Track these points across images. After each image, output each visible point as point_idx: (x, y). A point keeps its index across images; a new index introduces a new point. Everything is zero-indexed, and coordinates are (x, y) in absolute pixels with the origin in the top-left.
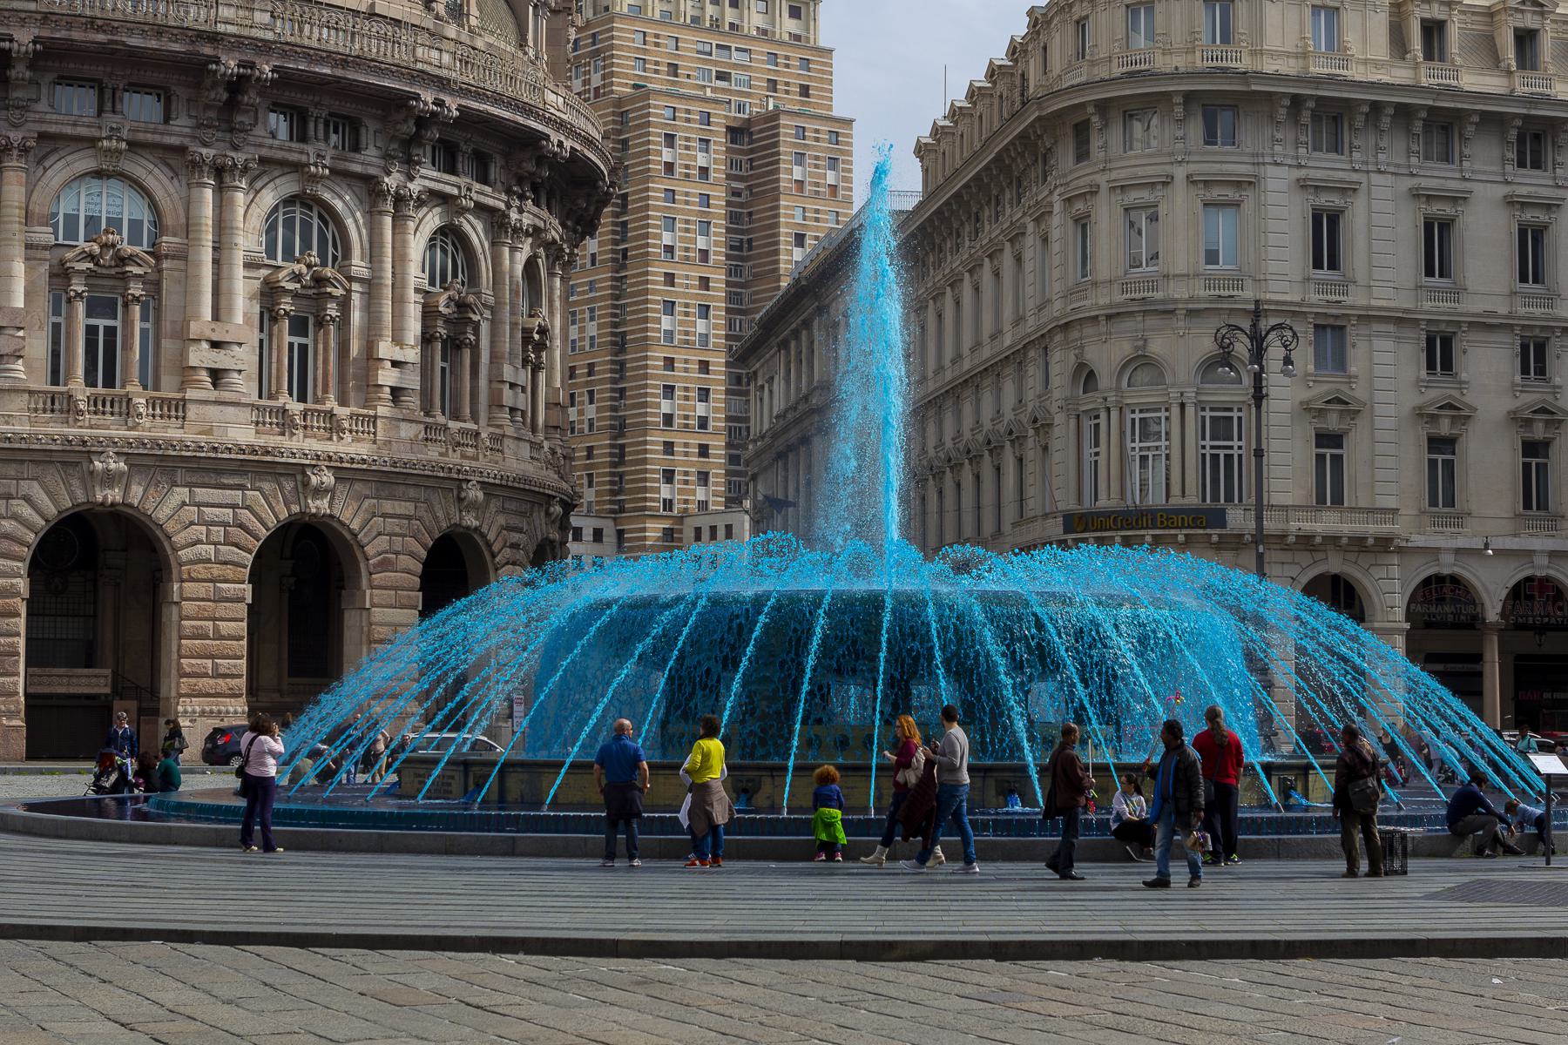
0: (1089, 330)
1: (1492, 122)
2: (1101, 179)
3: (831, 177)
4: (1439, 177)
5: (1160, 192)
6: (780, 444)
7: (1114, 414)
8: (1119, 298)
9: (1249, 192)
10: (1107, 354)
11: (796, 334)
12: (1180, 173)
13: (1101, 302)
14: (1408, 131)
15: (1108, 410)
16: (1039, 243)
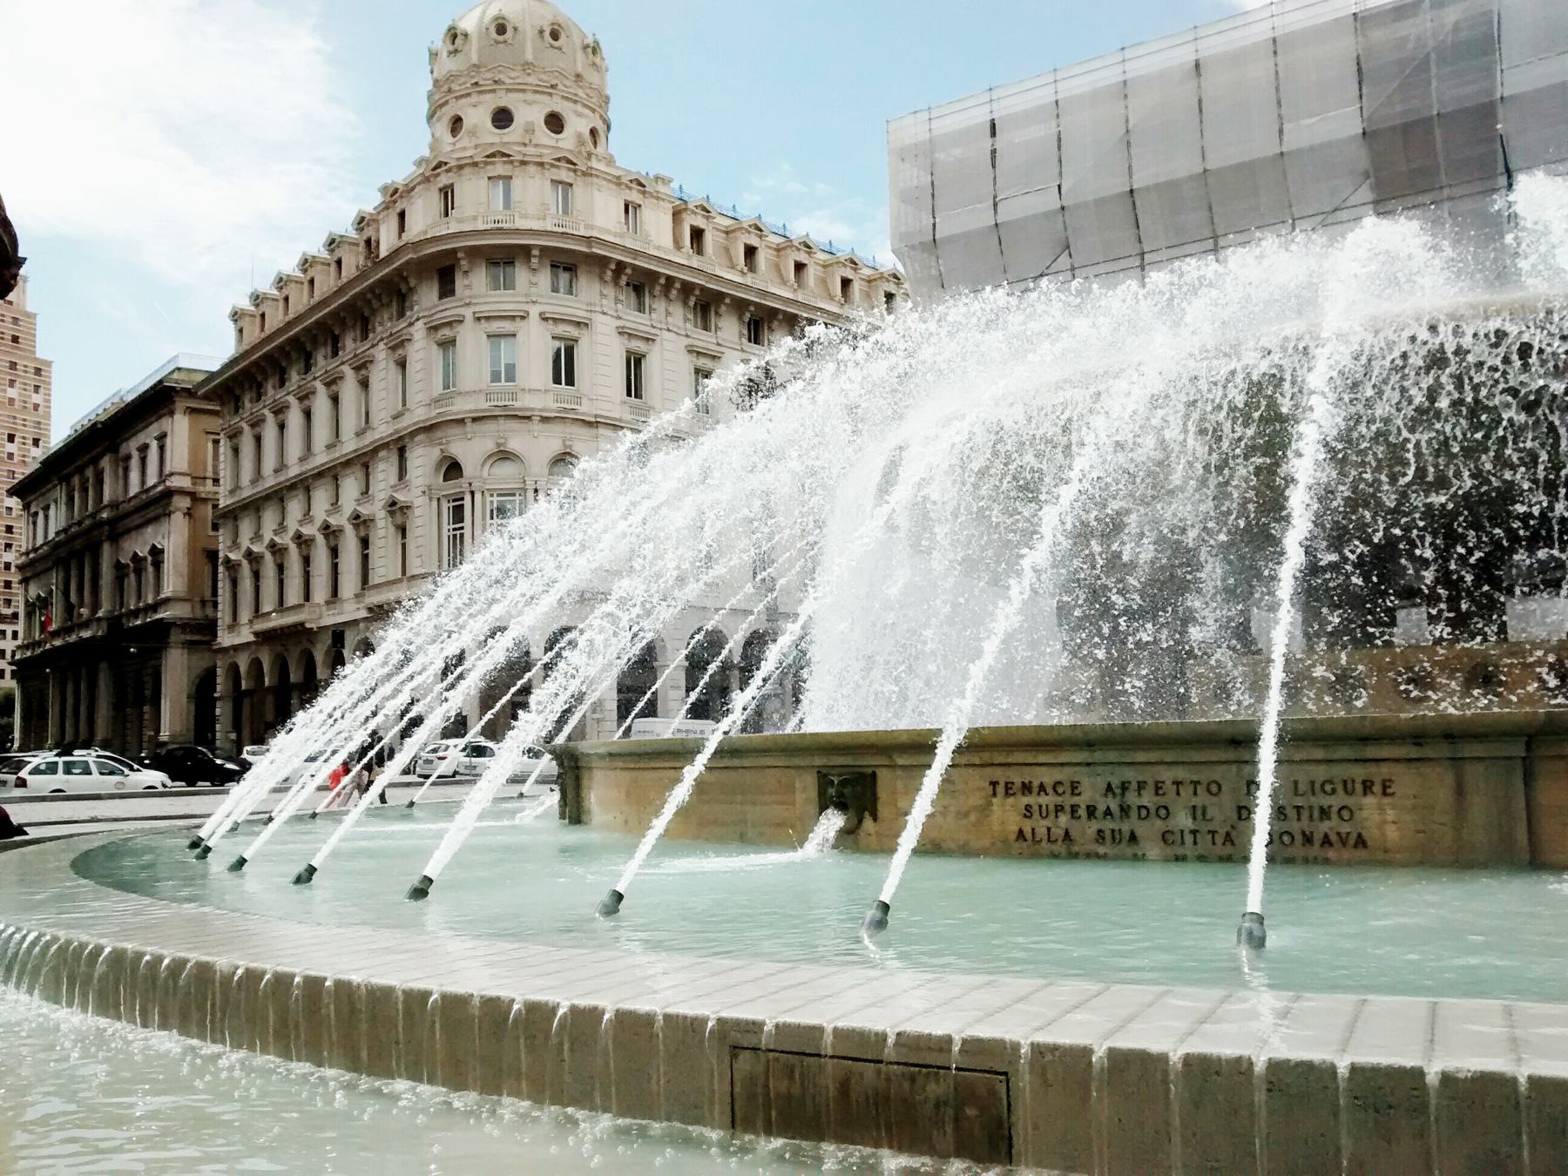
0: (455, 431)
1: (740, 305)
2: (468, 313)
3: (36, 398)
4: (704, 340)
5: (519, 323)
6: (63, 553)
7: (478, 496)
8: (486, 405)
9: (584, 332)
10: (470, 450)
11: (80, 470)
12: (534, 311)
13: (471, 406)
14: (685, 304)
15: (472, 493)
16: (392, 366)
